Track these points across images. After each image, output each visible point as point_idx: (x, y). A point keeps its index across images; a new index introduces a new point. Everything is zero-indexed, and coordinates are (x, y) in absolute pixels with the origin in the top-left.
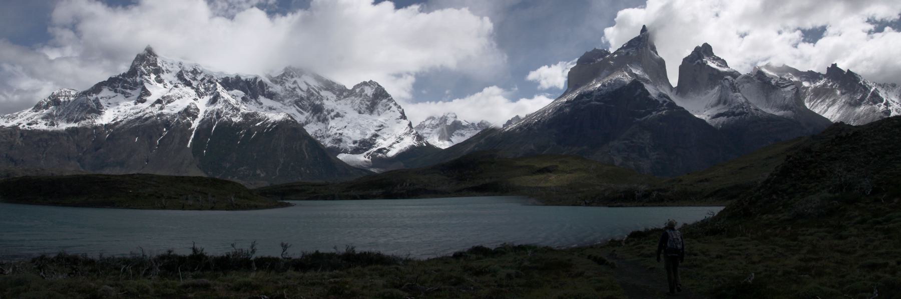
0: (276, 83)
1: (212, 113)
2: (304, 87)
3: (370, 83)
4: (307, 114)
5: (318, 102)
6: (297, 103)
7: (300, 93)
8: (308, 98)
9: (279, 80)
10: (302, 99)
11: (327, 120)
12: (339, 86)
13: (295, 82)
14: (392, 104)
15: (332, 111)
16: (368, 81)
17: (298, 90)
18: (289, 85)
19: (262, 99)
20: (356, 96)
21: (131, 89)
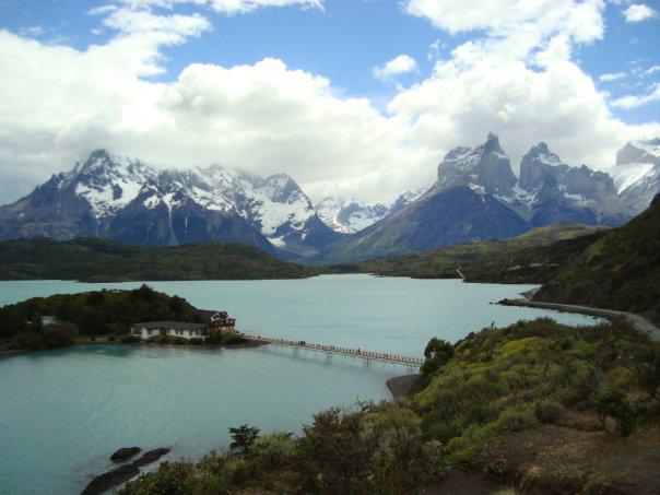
0: (204, 173)
2: (230, 180)
6: (224, 193)
7: (227, 185)
8: (233, 189)
10: (228, 190)
13: (222, 175)
14: (301, 195)
15: (253, 199)
16: (280, 173)
18: (217, 177)
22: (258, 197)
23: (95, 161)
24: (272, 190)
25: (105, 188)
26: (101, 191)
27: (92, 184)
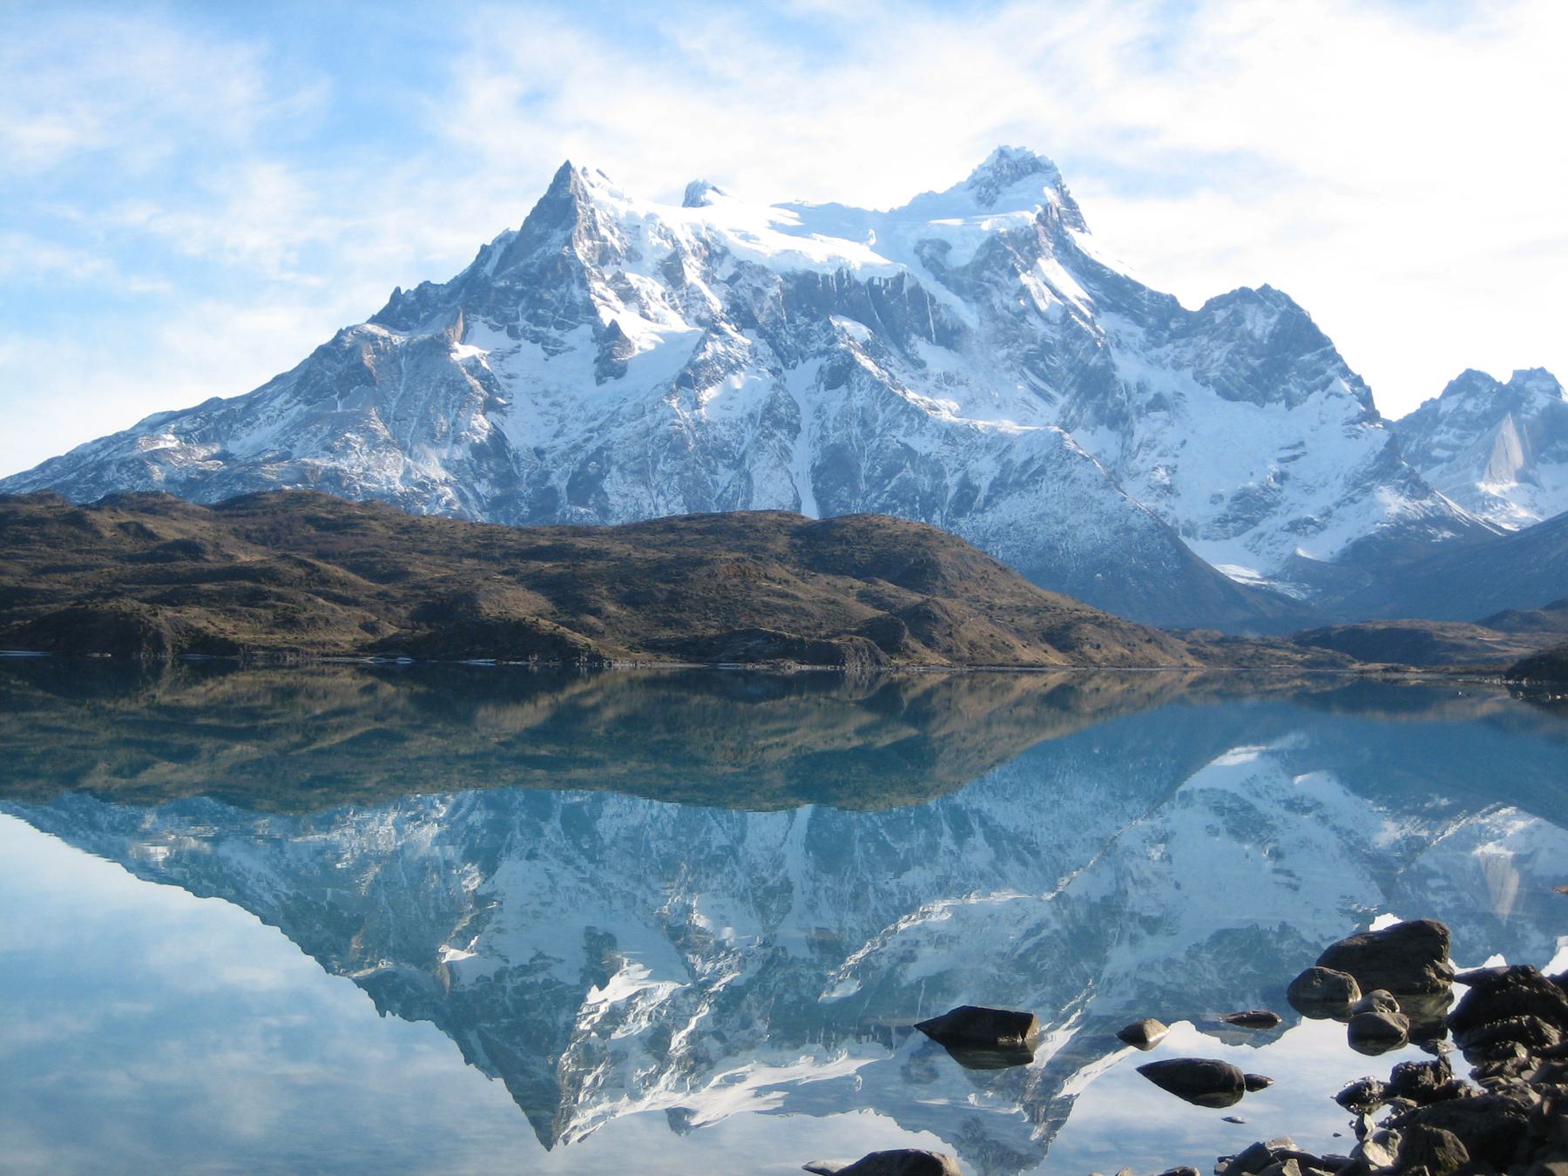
0: (959, 290)
1: (845, 418)
3: (1266, 297)
4: (1062, 401)
5: (1094, 360)
6: (1029, 361)
8: (1065, 347)
9: (967, 280)
10: (1046, 349)
11: (1126, 418)
12: (1155, 296)
15: (1141, 388)
16: (1255, 286)
17: (1032, 319)
19: (922, 348)
20: (1214, 333)
21: (560, 326)
22: (1163, 381)
23: (542, 239)
24: (1220, 353)
25: (571, 338)
26: (553, 350)
27: (522, 323)
